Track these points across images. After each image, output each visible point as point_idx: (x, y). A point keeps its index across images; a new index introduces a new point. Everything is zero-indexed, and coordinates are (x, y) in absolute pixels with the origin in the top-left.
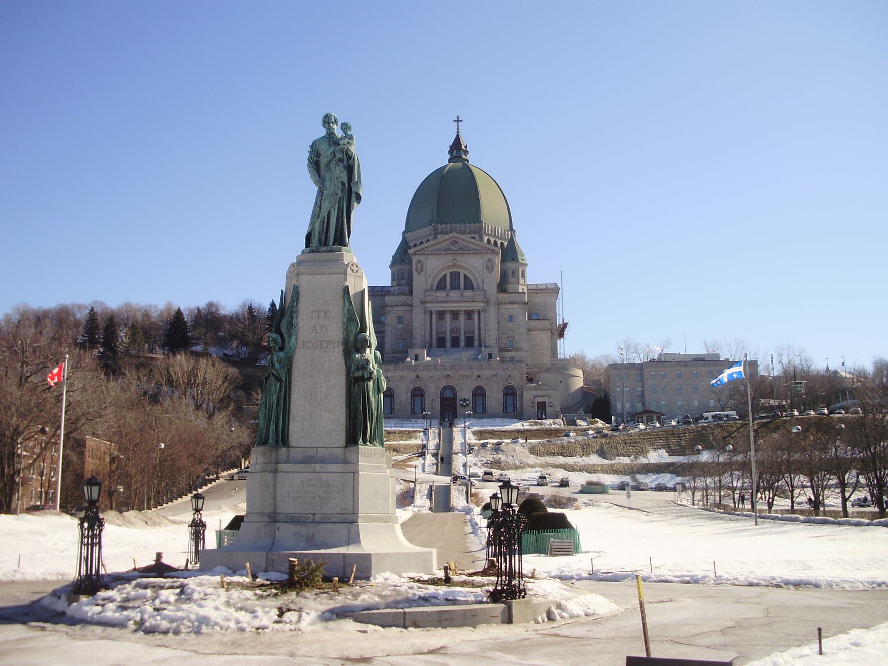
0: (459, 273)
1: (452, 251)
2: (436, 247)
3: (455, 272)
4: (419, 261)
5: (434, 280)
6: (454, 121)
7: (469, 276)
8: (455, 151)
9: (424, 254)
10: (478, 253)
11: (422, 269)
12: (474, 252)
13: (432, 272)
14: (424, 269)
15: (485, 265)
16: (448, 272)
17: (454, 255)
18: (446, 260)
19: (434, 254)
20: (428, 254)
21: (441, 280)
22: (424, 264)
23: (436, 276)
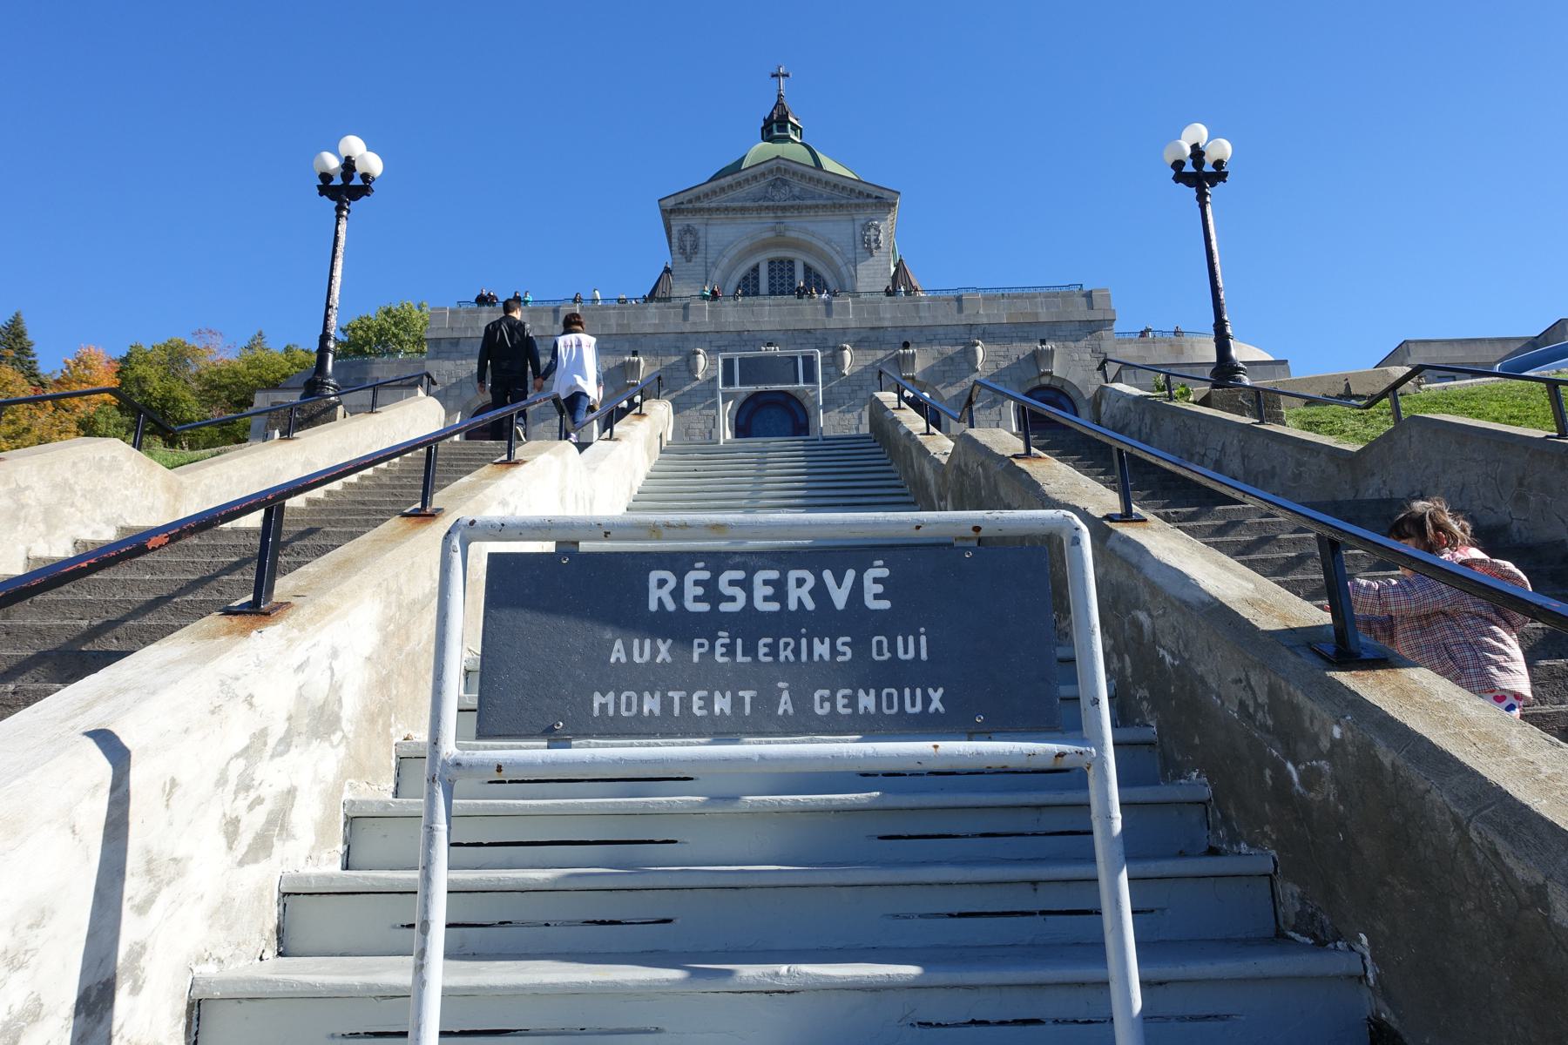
0: (791, 262)
1: (773, 201)
2: (731, 194)
3: (781, 262)
4: (689, 230)
5: (726, 278)
6: (773, 76)
7: (819, 267)
8: (775, 126)
9: (701, 210)
10: (841, 206)
11: (695, 247)
12: (830, 202)
13: (721, 253)
14: (702, 247)
15: (858, 237)
16: (762, 259)
17: (780, 214)
18: (755, 228)
19: (726, 209)
20: (709, 210)
21: (745, 278)
22: (701, 234)
23: (733, 267)
